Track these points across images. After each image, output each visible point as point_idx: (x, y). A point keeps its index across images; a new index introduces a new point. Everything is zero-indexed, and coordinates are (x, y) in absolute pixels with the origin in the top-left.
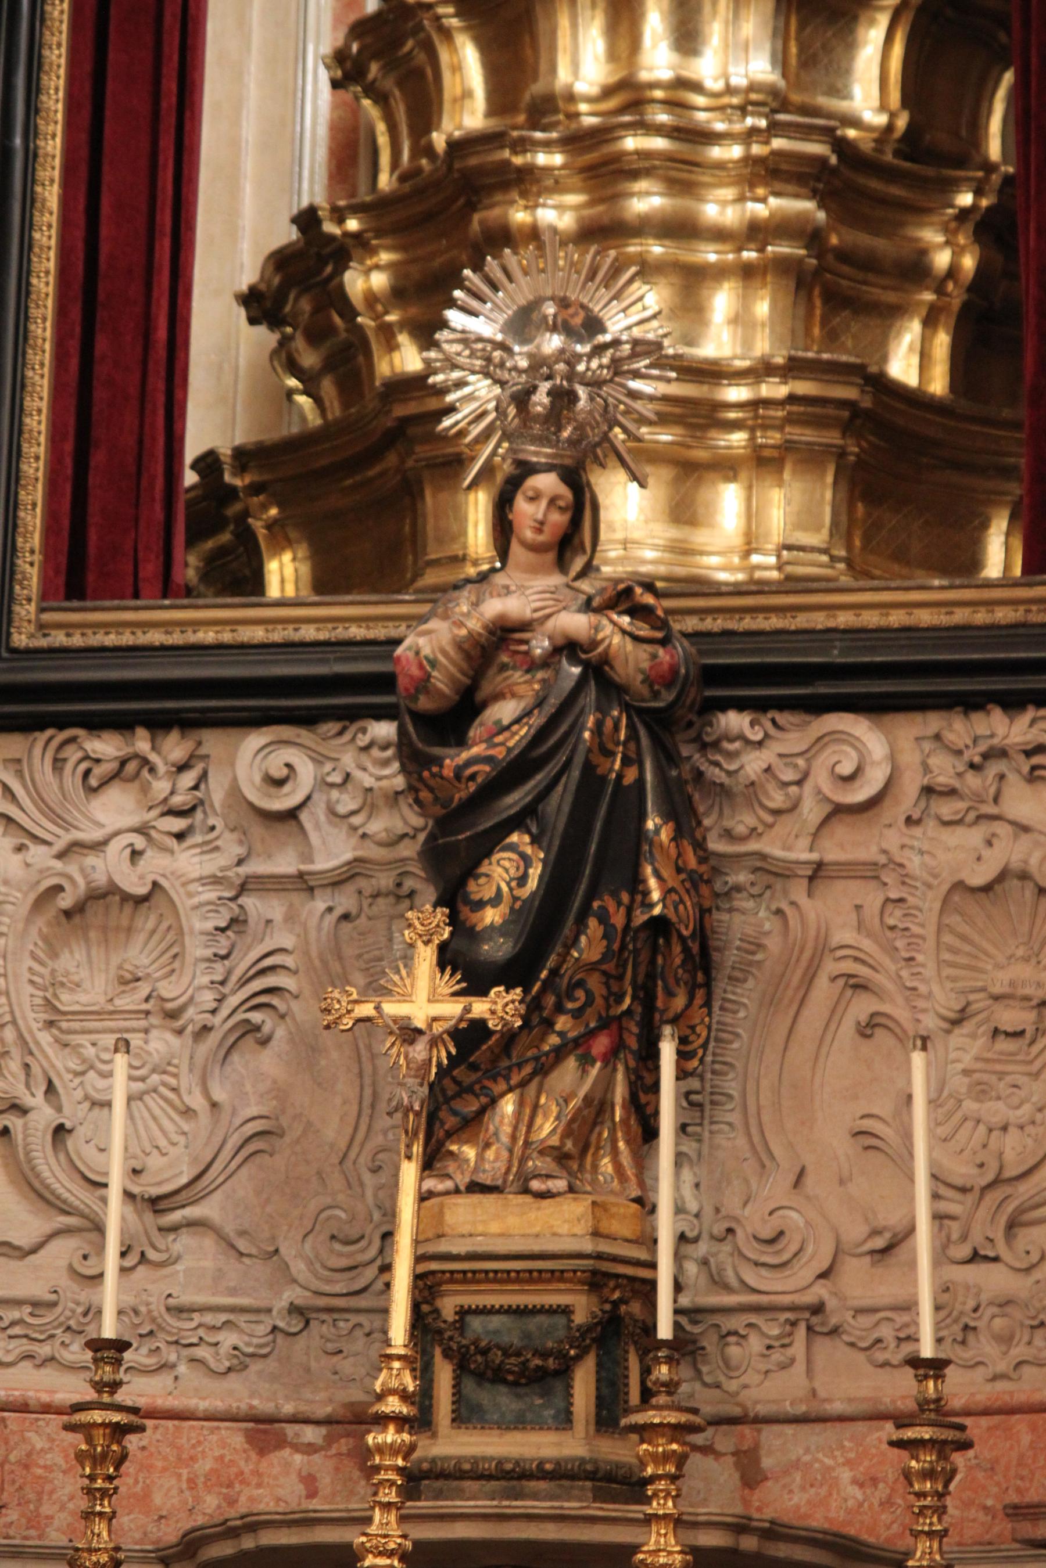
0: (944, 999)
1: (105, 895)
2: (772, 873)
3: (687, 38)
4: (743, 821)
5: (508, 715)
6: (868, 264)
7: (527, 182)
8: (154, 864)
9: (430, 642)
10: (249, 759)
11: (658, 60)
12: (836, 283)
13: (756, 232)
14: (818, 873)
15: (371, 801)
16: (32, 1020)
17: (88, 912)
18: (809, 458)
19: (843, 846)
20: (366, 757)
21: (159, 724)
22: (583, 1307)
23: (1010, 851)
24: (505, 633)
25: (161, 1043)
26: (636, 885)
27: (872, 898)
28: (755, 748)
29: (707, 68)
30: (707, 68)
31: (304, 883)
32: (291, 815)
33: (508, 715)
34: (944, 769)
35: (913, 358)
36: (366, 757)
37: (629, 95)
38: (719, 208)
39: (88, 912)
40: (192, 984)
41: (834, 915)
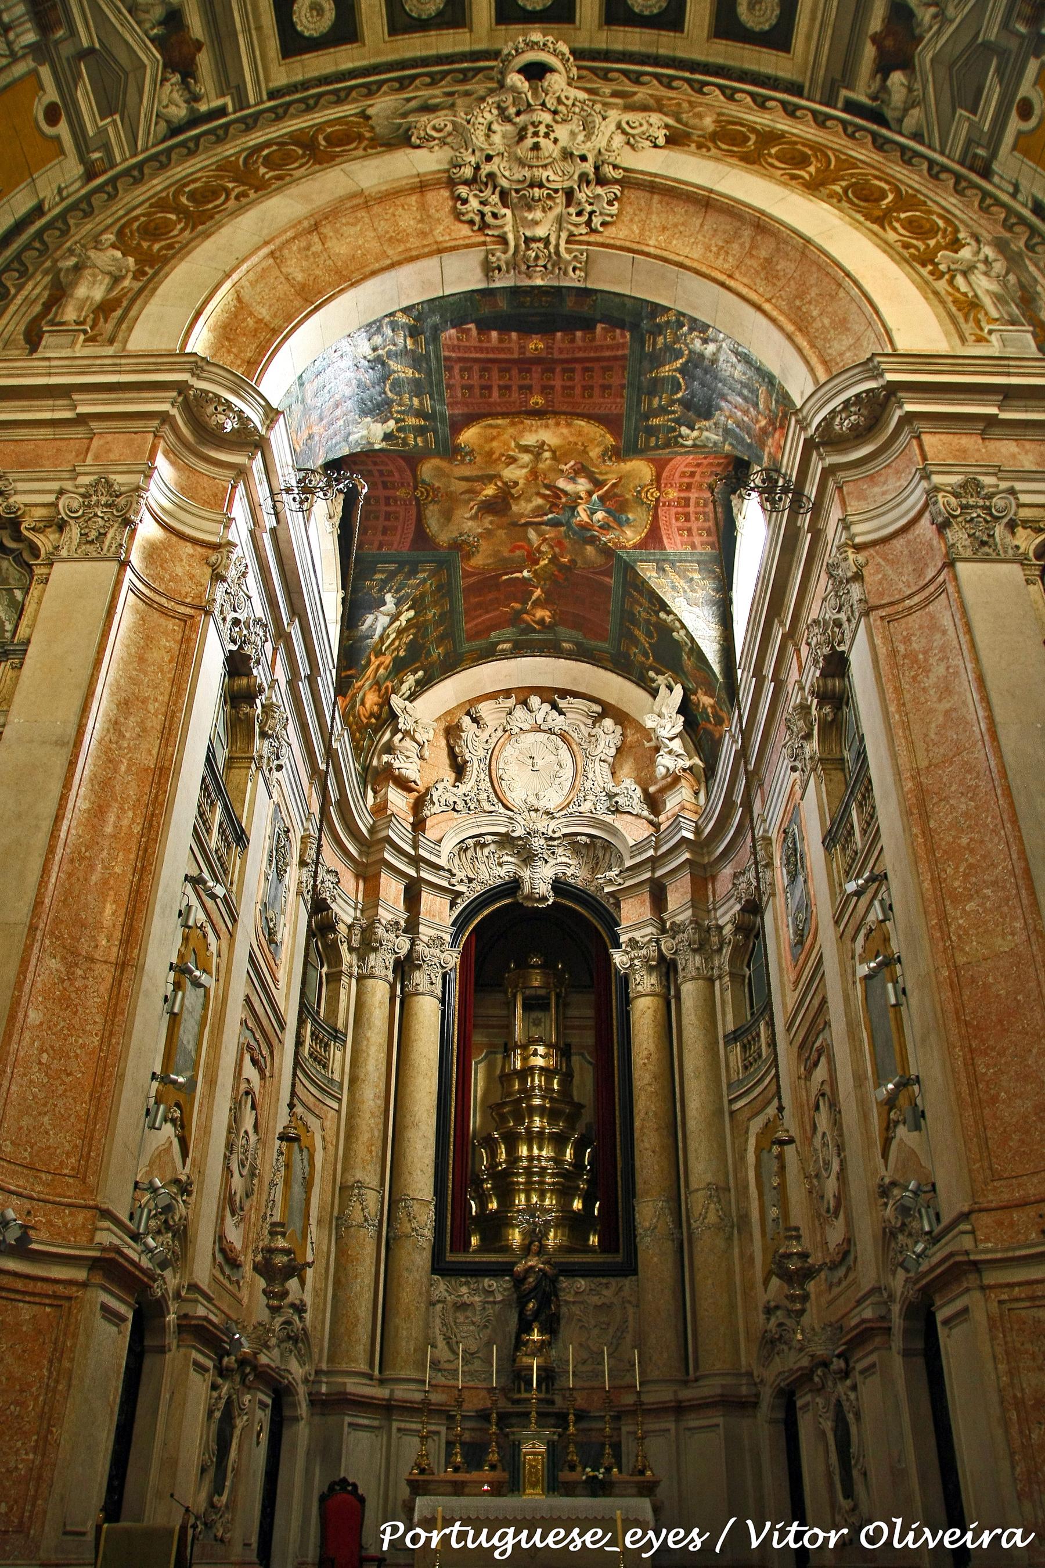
0: (593, 1322)
1: (464, 1304)
2: (567, 1302)
3: (540, 1149)
6: (570, 1188)
7: (518, 1175)
8: (472, 1299)
9: (519, 1268)
10: (486, 1281)
11: (536, 1152)
12: (565, 1193)
13: (553, 1184)
14: (574, 1303)
15: (505, 1290)
18: (564, 1226)
19: (579, 1299)
20: (506, 1282)
21: (472, 1276)
23: (603, 1300)
24: (531, 1267)
25: (472, 1328)
28: (564, 1283)
29: (544, 1153)
30: (544, 1153)
31: (495, 1303)
34: (593, 1286)
35: (577, 1205)
36: (506, 1282)
37: (531, 1158)
38: (548, 1180)
41: (576, 1310)
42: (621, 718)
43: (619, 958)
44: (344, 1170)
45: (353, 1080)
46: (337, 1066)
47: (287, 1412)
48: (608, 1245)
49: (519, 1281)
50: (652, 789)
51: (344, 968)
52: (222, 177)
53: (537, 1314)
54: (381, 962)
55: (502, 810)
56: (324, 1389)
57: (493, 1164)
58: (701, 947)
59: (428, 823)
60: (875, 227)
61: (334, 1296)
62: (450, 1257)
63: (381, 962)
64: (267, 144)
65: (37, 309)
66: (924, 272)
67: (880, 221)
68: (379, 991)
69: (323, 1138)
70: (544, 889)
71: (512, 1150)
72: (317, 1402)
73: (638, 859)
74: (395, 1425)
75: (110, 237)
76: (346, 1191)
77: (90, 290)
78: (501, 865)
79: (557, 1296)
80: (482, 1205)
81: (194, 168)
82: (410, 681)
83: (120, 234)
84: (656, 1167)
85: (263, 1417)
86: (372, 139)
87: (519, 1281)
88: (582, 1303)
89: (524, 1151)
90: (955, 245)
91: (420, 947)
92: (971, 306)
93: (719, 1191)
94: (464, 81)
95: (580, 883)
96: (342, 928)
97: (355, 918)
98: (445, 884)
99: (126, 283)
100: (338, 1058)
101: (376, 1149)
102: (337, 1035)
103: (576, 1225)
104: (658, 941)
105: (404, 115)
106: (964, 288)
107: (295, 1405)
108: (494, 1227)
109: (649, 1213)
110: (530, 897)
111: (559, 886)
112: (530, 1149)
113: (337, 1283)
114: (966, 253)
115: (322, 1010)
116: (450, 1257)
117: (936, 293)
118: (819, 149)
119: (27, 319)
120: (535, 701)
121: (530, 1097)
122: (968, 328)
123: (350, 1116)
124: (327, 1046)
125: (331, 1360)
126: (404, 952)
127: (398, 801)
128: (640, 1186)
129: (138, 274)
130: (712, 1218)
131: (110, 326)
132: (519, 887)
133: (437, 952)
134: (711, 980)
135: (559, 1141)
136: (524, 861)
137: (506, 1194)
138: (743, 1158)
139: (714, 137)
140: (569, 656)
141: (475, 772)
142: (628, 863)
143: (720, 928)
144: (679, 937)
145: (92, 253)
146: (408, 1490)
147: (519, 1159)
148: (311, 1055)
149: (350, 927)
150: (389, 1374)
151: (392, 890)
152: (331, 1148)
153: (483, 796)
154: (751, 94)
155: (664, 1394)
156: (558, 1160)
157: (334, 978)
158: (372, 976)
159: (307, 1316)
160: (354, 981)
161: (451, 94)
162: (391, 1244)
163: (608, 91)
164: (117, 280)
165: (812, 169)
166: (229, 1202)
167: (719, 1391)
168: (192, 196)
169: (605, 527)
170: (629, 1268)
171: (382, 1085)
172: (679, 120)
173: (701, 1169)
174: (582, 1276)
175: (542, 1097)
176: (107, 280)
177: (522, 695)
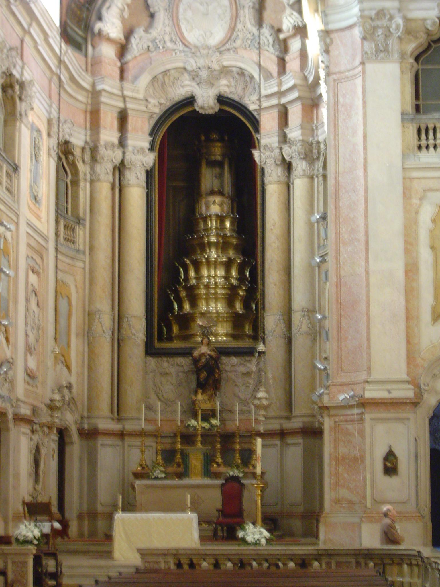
4: (224, 366)
5: (203, 360)
9: (196, 354)
14: (230, 372)
16: (160, 385)
17: (164, 374)
19: (233, 369)
22: (211, 413)
26: (214, 376)
27: (235, 374)
32: (183, 366)
33: (203, 360)
34: (242, 362)
35: (239, 307)
37: (209, 277)
39: (164, 374)
40: (174, 381)
44: (90, 302)
45: (92, 249)
46: (81, 241)
47: (67, 440)
49: (196, 361)
50: (282, 36)
51: (81, 176)
53: (207, 380)
55: (181, 47)
56: (86, 426)
57: (187, 278)
59: (131, 65)
61: (89, 376)
62: (157, 345)
68: (104, 190)
69: (76, 286)
71: (197, 270)
72: (82, 433)
73: (269, 92)
74: (126, 443)
76: (90, 315)
78: (183, 87)
79: (218, 368)
80: (180, 307)
84: (276, 294)
85: (54, 446)
87: (196, 361)
88: (235, 371)
89: (205, 272)
91: (129, 157)
93: (310, 312)
95: (237, 98)
96: (77, 152)
97: (86, 142)
98: (144, 108)
100: (81, 234)
101: (108, 289)
102: (79, 221)
103: (237, 321)
104: (281, 149)
107: (70, 436)
109: (272, 321)
110: (202, 108)
111: (221, 99)
112: (209, 271)
113: (90, 368)
115: (70, 206)
116: (157, 345)
121: (208, 236)
123: (92, 271)
124: (74, 230)
125: (89, 409)
126: (117, 162)
127: (108, 52)
128: (267, 305)
130: (304, 328)
132: (195, 100)
133: (140, 157)
134: (312, 178)
135: (228, 265)
136: (198, 84)
137: (194, 301)
138: (323, 293)
141: (161, 17)
142: (264, 92)
143: (318, 143)
144: (294, 148)
146: (132, 477)
147: (203, 277)
148: (65, 239)
149: (83, 149)
150: (123, 415)
152: (80, 291)
153: (167, 38)
155: (275, 425)
156: (227, 278)
157: (75, 183)
158: (99, 180)
159: (74, 390)
160: (88, 185)
162: (119, 343)
166: (29, 350)
167: (300, 425)
171: (109, 250)
173: (300, 299)
174: (235, 356)
175: (218, 235)
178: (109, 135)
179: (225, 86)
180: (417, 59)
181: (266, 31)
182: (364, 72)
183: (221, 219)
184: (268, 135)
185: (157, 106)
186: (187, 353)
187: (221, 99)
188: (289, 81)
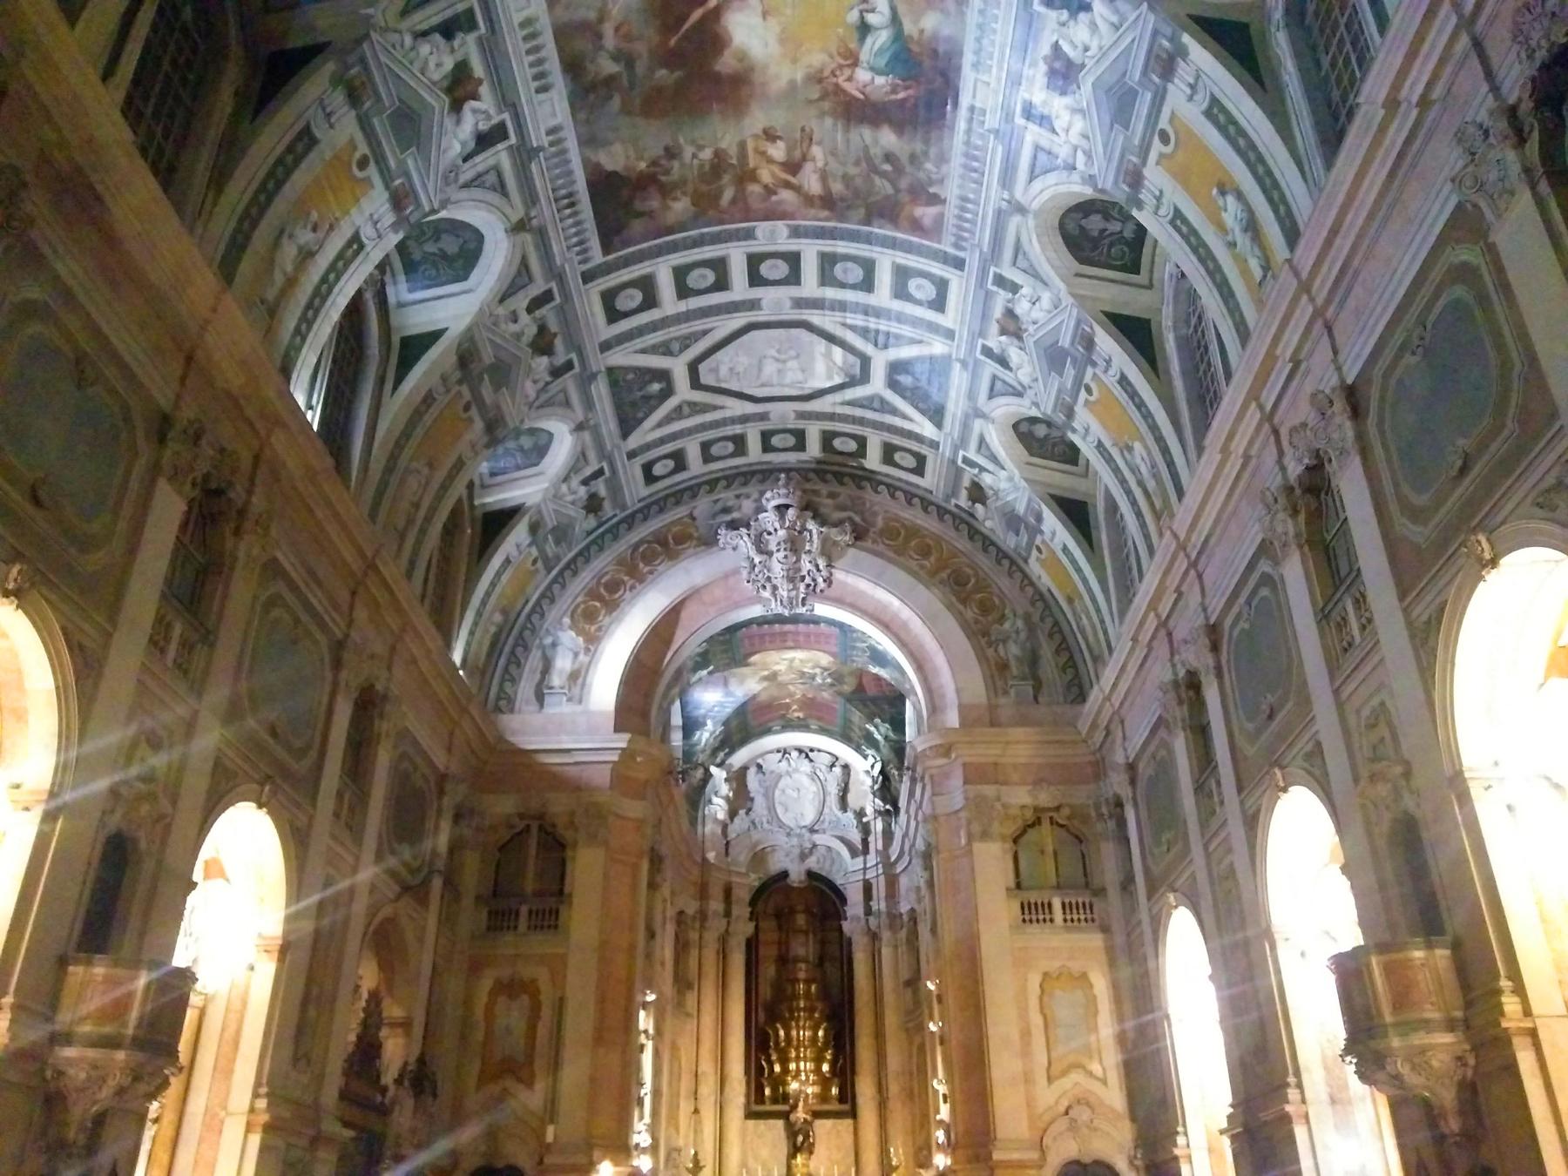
12: (818, 1060)
42: (846, 767)
43: (846, 926)
48: (842, 1098)
52: (618, 571)
54: (711, 937)
58: (891, 927)
60: (961, 607)
63: (711, 937)
64: (641, 542)
65: (538, 676)
66: (983, 641)
67: (964, 602)
70: (803, 878)
75: (567, 620)
77: (563, 664)
80: (771, 1070)
81: (603, 563)
82: (722, 755)
83: (572, 617)
86: (699, 539)
89: (794, 1033)
90: (1002, 619)
92: (1003, 667)
94: (745, 484)
99: (582, 657)
103: (824, 1082)
105: (714, 516)
106: (1002, 653)
108: (779, 1082)
114: (1007, 625)
117: (987, 659)
118: (939, 539)
119: (534, 684)
120: (795, 754)
122: (999, 683)
129: (587, 650)
131: (576, 691)
137: (784, 1062)
139: (882, 533)
140: (815, 732)
145: (560, 634)
151: (716, 891)
154: (905, 492)
161: (738, 497)
163: (824, 492)
164: (576, 655)
165: (932, 559)
168: (606, 586)
169: (832, 685)
170: (853, 1114)
172: (863, 520)
176: (571, 655)
177: (785, 752)
178: (716, 905)
179: (812, 863)
180: (1015, 841)
181: (850, 815)
182: (971, 852)
183: (808, 982)
184: (855, 907)
185: (754, 880)
186: (785, 1116)
187: (811, 875)
188: (872, 859)
